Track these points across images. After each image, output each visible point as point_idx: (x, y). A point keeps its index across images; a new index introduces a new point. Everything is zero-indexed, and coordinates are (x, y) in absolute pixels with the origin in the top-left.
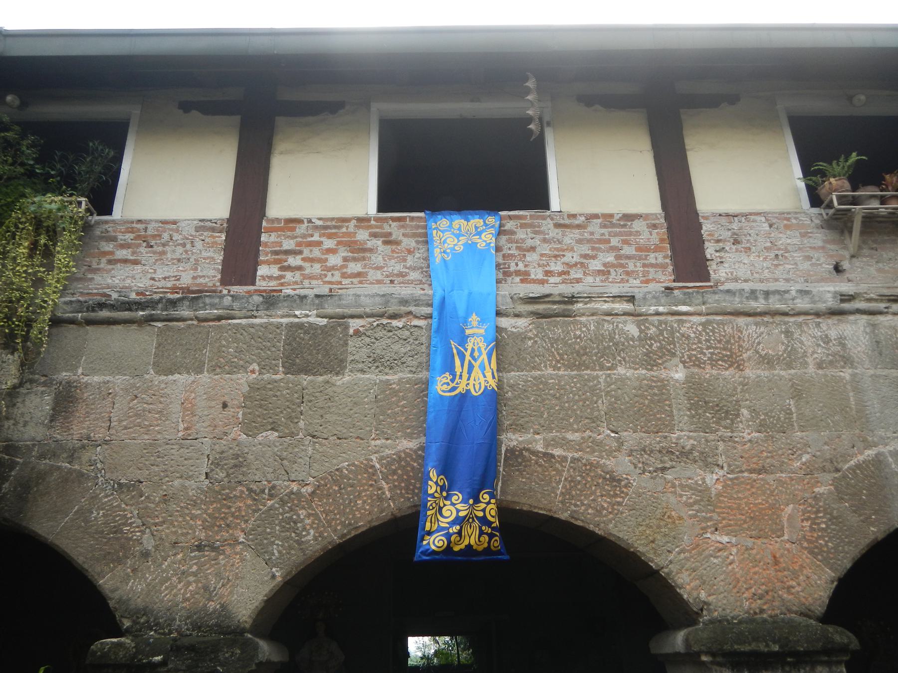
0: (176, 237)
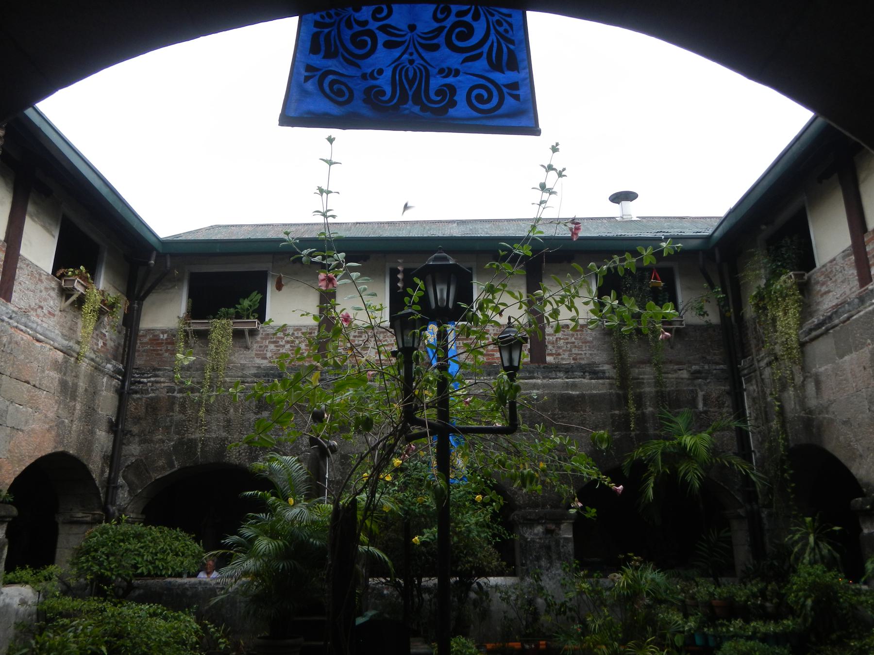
0: (838, 267)
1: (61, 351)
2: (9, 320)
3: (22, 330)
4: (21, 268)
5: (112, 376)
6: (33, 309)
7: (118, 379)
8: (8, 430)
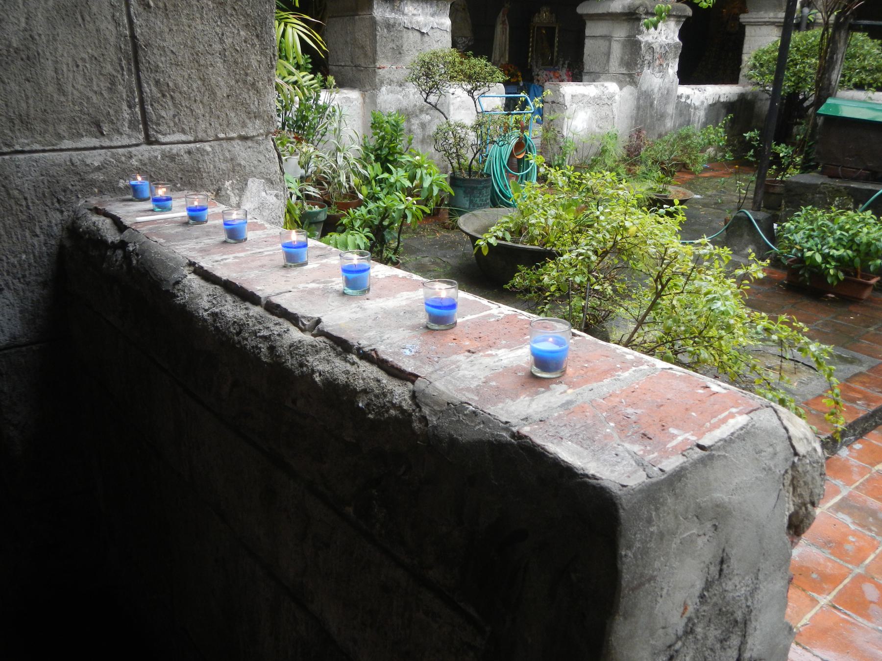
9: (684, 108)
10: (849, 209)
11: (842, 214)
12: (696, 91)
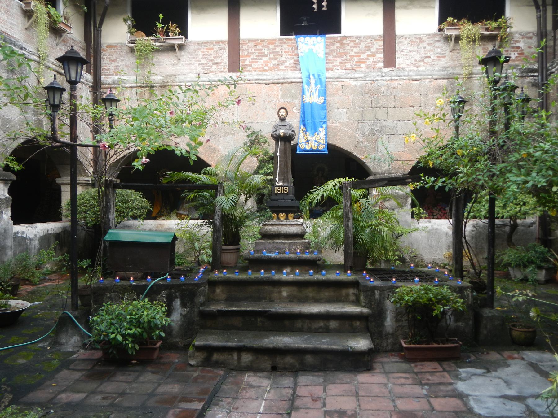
1: (444, 79)
2: (383, 78)
3: (397, 80)
4: (400, 42)
5: (522, 77)
6: (419, 61)
7: (534, 76)
8: (401, 136)
9: (21, 241)
10: (134, 300)
11: (130, 304)
12: (30, 228)
